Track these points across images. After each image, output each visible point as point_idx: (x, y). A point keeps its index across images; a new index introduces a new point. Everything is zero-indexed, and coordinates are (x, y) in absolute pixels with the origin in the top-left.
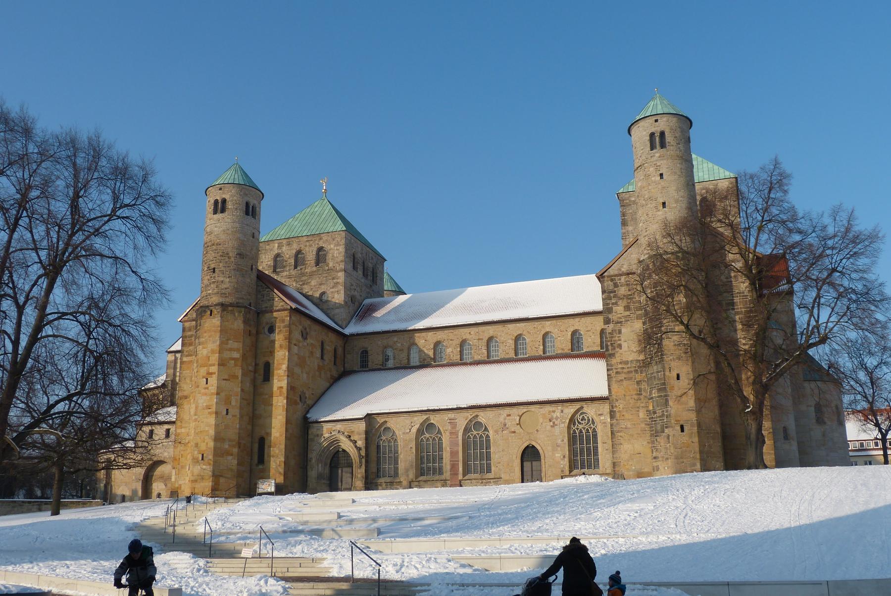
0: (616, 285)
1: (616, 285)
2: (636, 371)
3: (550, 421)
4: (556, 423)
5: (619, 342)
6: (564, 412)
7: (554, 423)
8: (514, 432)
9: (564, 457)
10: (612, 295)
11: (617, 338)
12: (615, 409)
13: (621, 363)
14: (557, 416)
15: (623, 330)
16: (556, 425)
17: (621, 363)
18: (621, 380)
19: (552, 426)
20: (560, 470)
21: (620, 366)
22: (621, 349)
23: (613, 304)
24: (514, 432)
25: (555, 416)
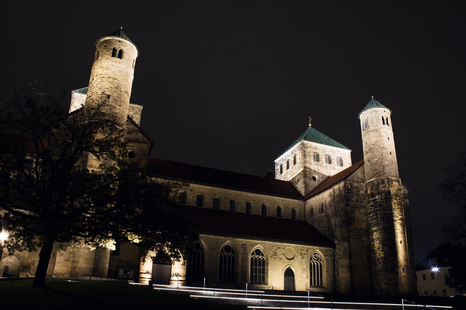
0: (352, 187)
1: (352, 187)
2: (362, 235)
3: (301, 255)
4: (304, 257)
5: (353, 218)
6: (308, 251)
7: (303, 256)
8: (281, 259)
9: (307, 277)
10: (350, 192)
11: (352, 215)
12: (352, 254)
13: (354, 229)
14: (304, 253)
15: (356, 212)
16: (304, 258)
17: (354, 229)
18: (355, 239)
19: (302, 258)
20: (305, 285)
21: (354, 231)
22: (355, 222)
23: (351, 196)
24: (281, 259)
25: (303, 253)
